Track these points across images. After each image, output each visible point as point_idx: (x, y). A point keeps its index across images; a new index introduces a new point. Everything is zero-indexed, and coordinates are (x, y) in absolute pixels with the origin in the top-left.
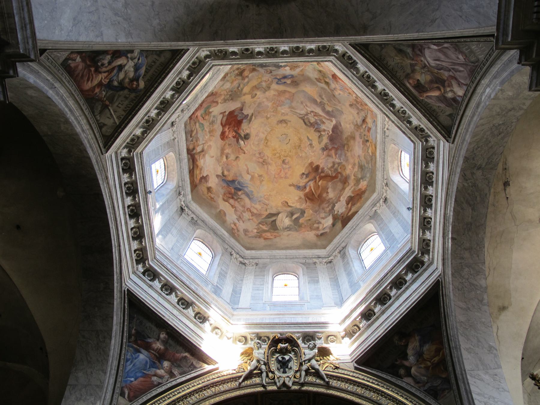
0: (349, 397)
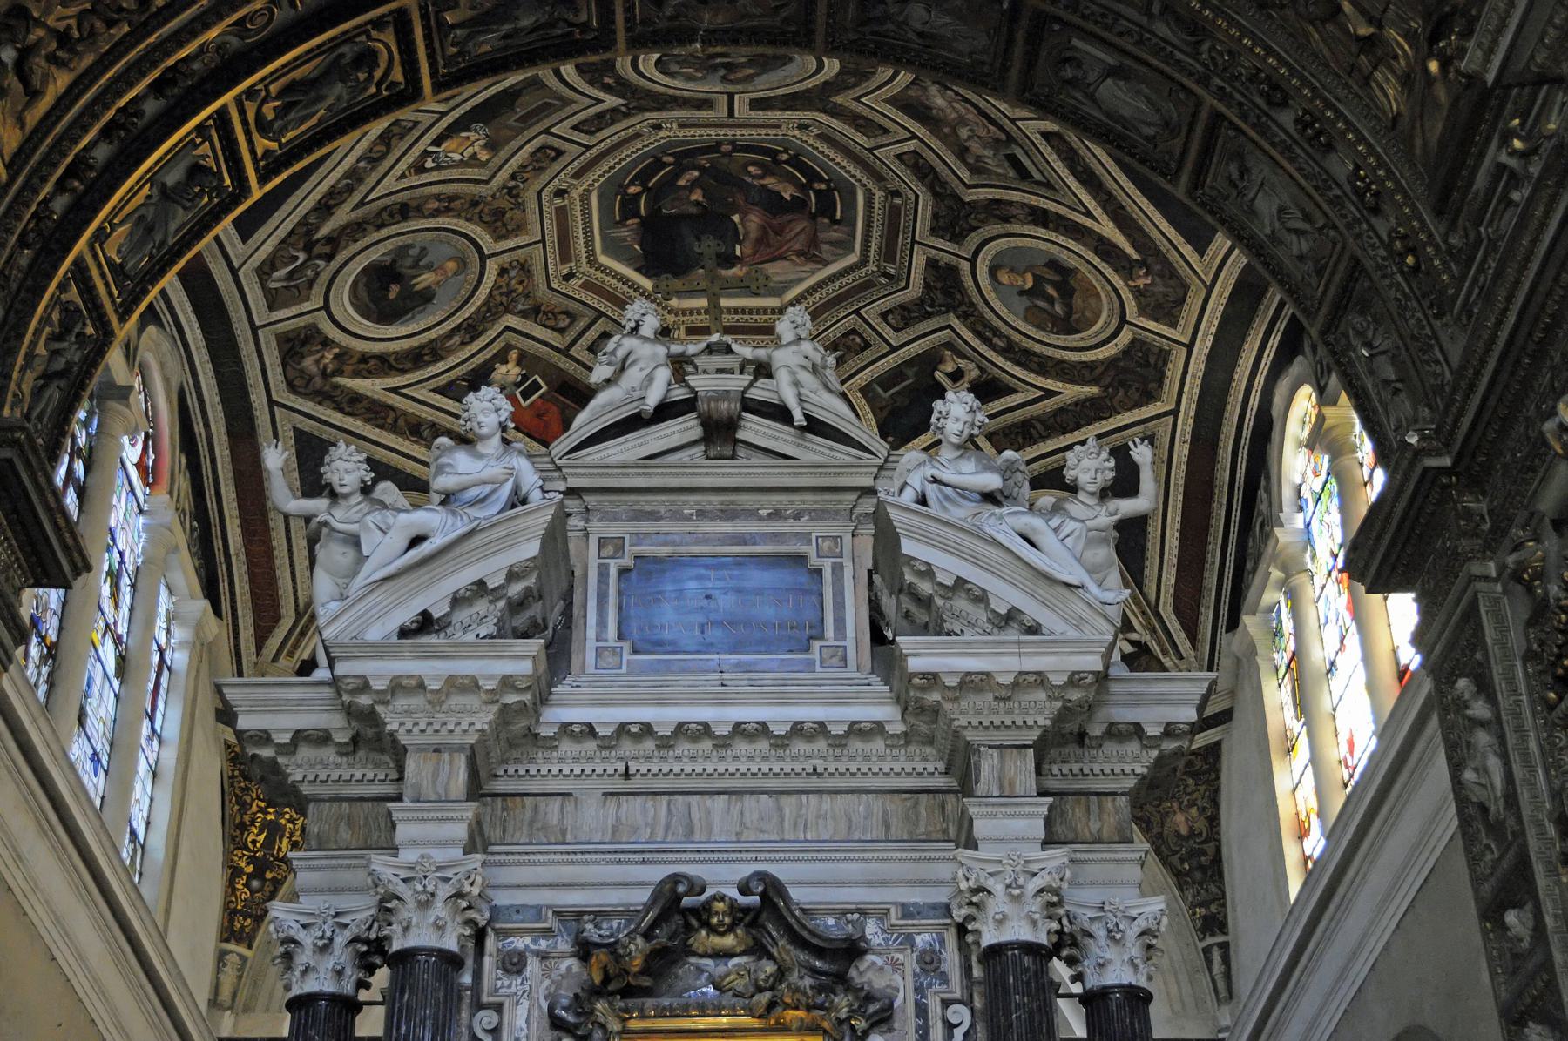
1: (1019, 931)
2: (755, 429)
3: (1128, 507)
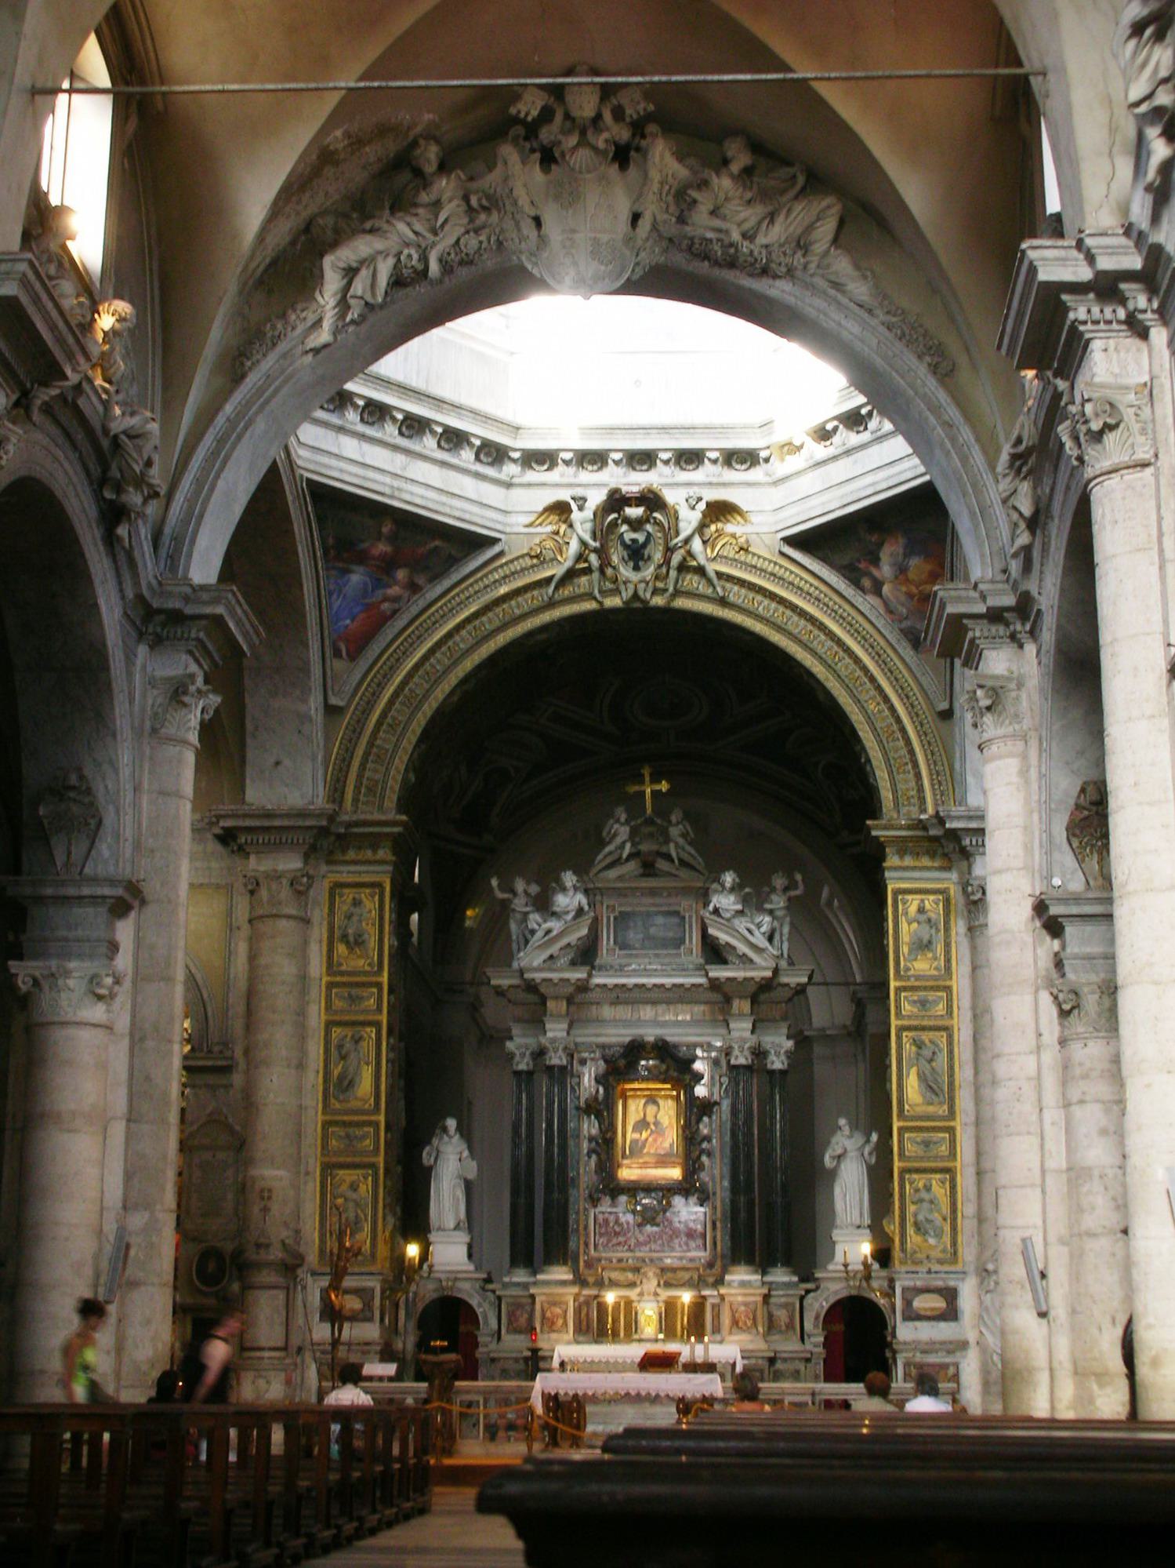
0: (758, 628)
1: (742, 1061)
2: (662, 865)
3: (793, 893)
